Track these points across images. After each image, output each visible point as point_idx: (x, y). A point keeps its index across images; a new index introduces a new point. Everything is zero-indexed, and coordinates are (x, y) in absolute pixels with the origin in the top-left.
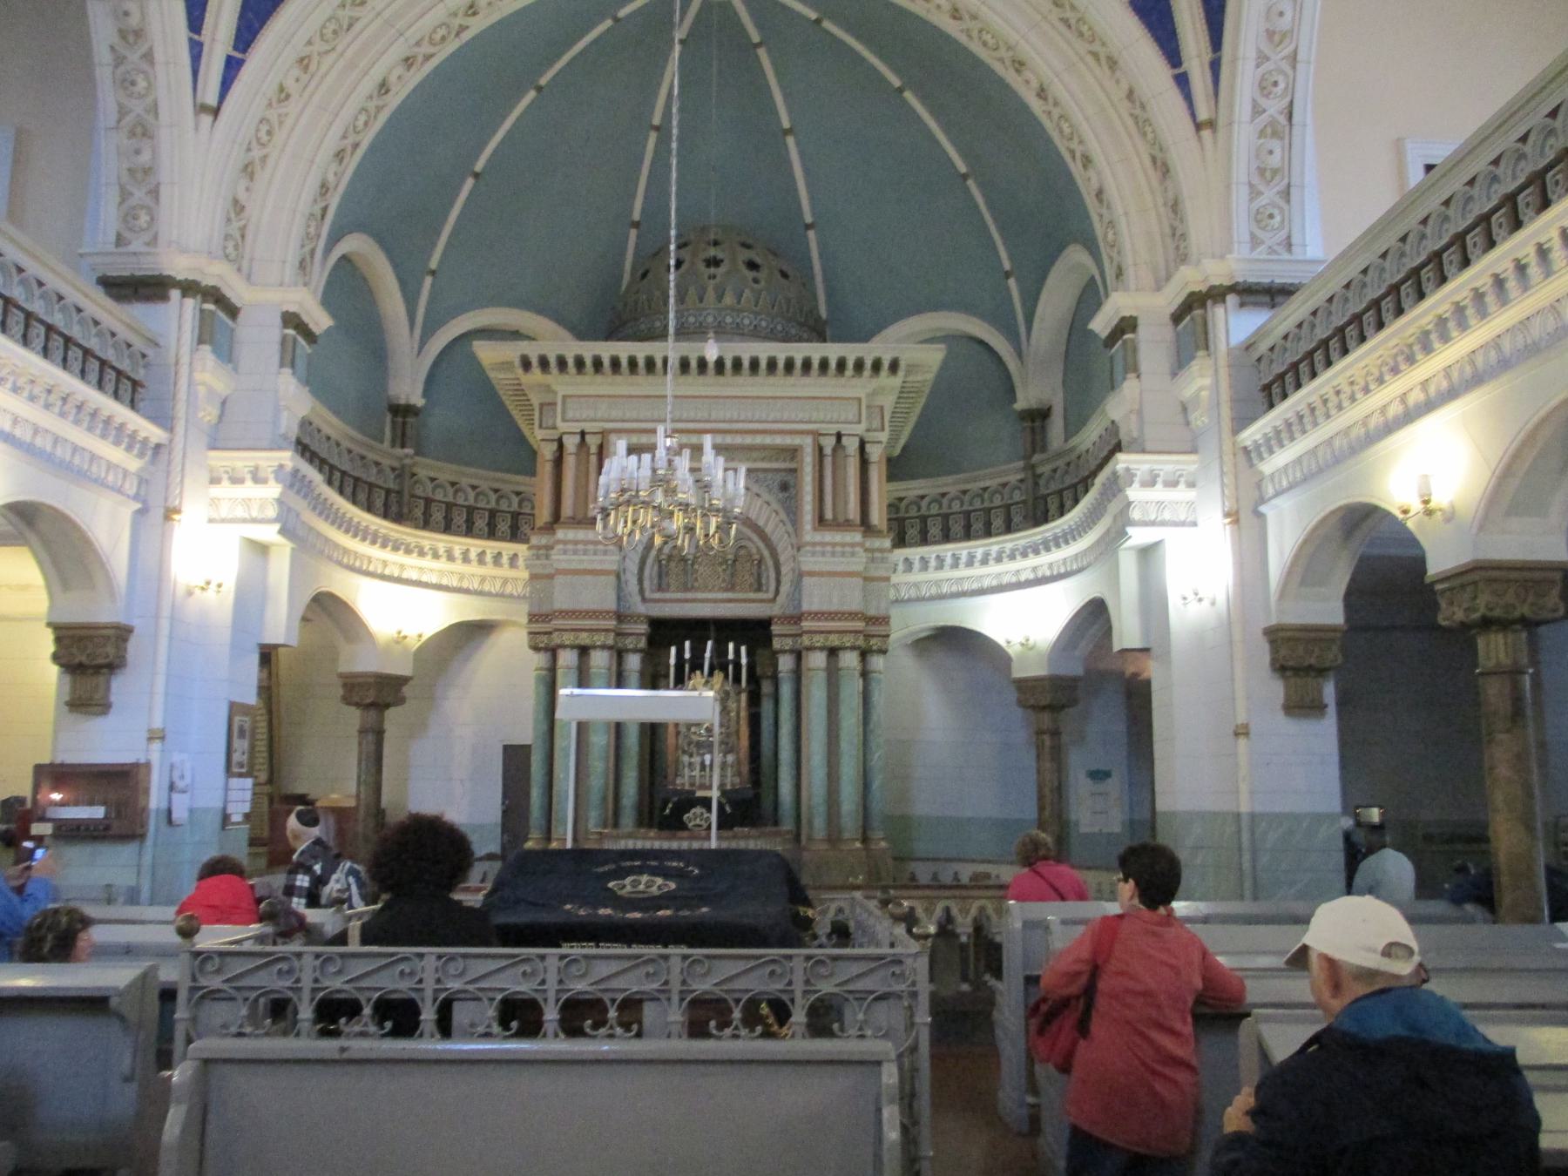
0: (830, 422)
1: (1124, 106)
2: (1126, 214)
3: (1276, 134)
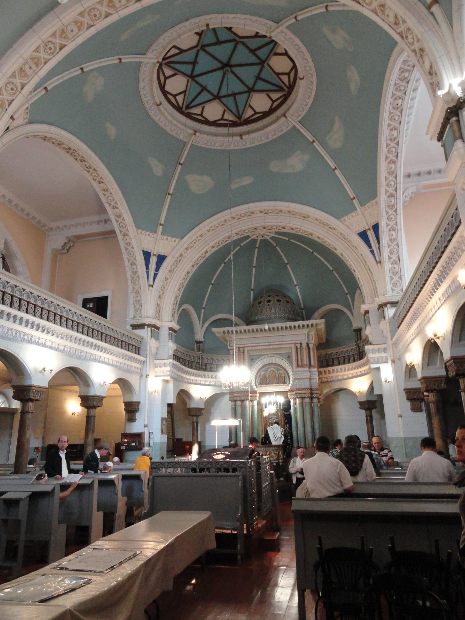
3: (396, 263)
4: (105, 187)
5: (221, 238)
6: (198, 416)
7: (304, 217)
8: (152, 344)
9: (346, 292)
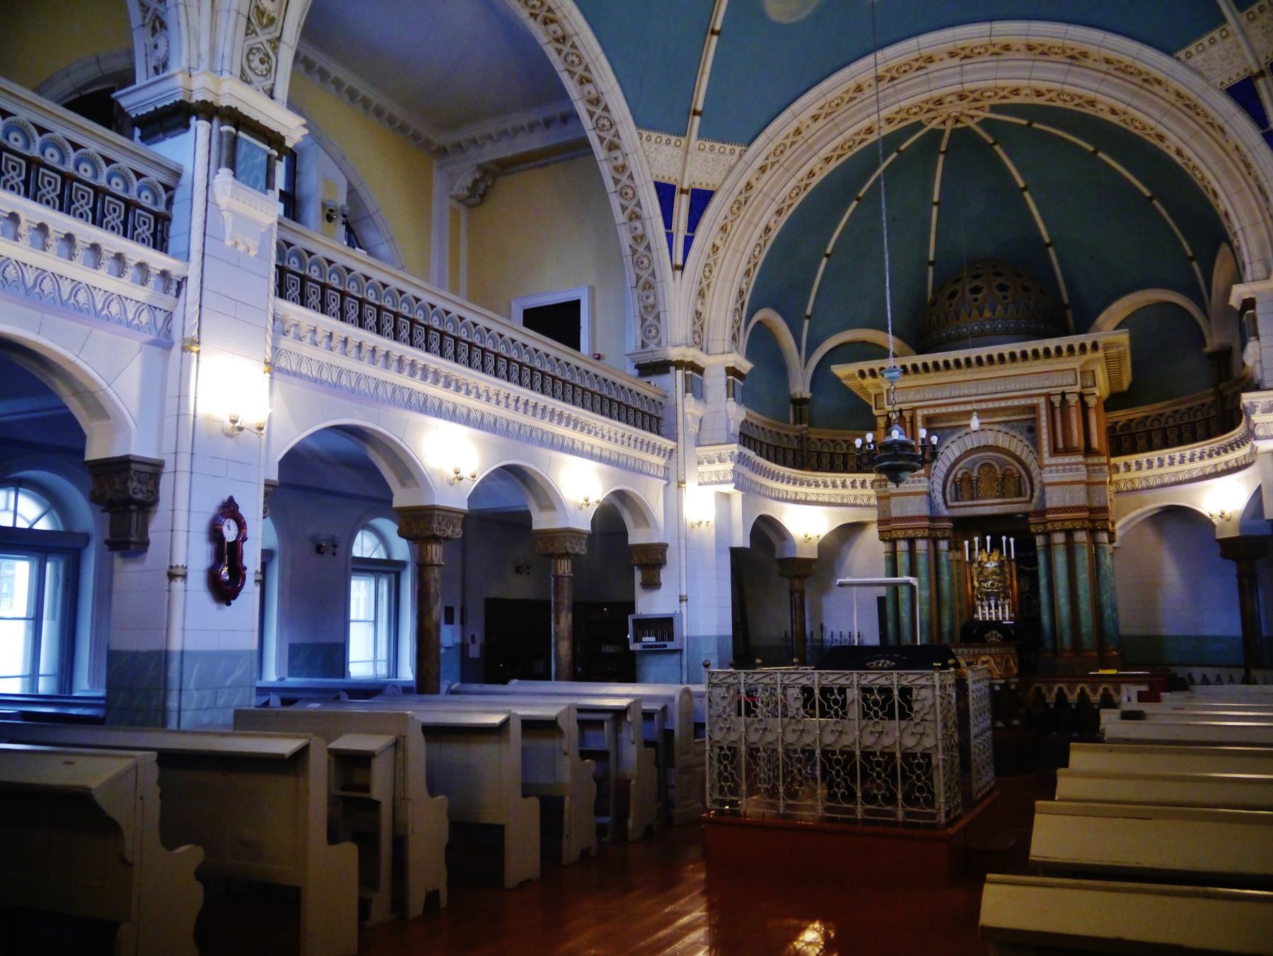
0: (1056, 387)
1: (1235, 155)
2: (1242, 229)
4: (560, 33)
5: (847, 134)
6: (802, 577)
7: (1072, 57)
8: (689, 409)
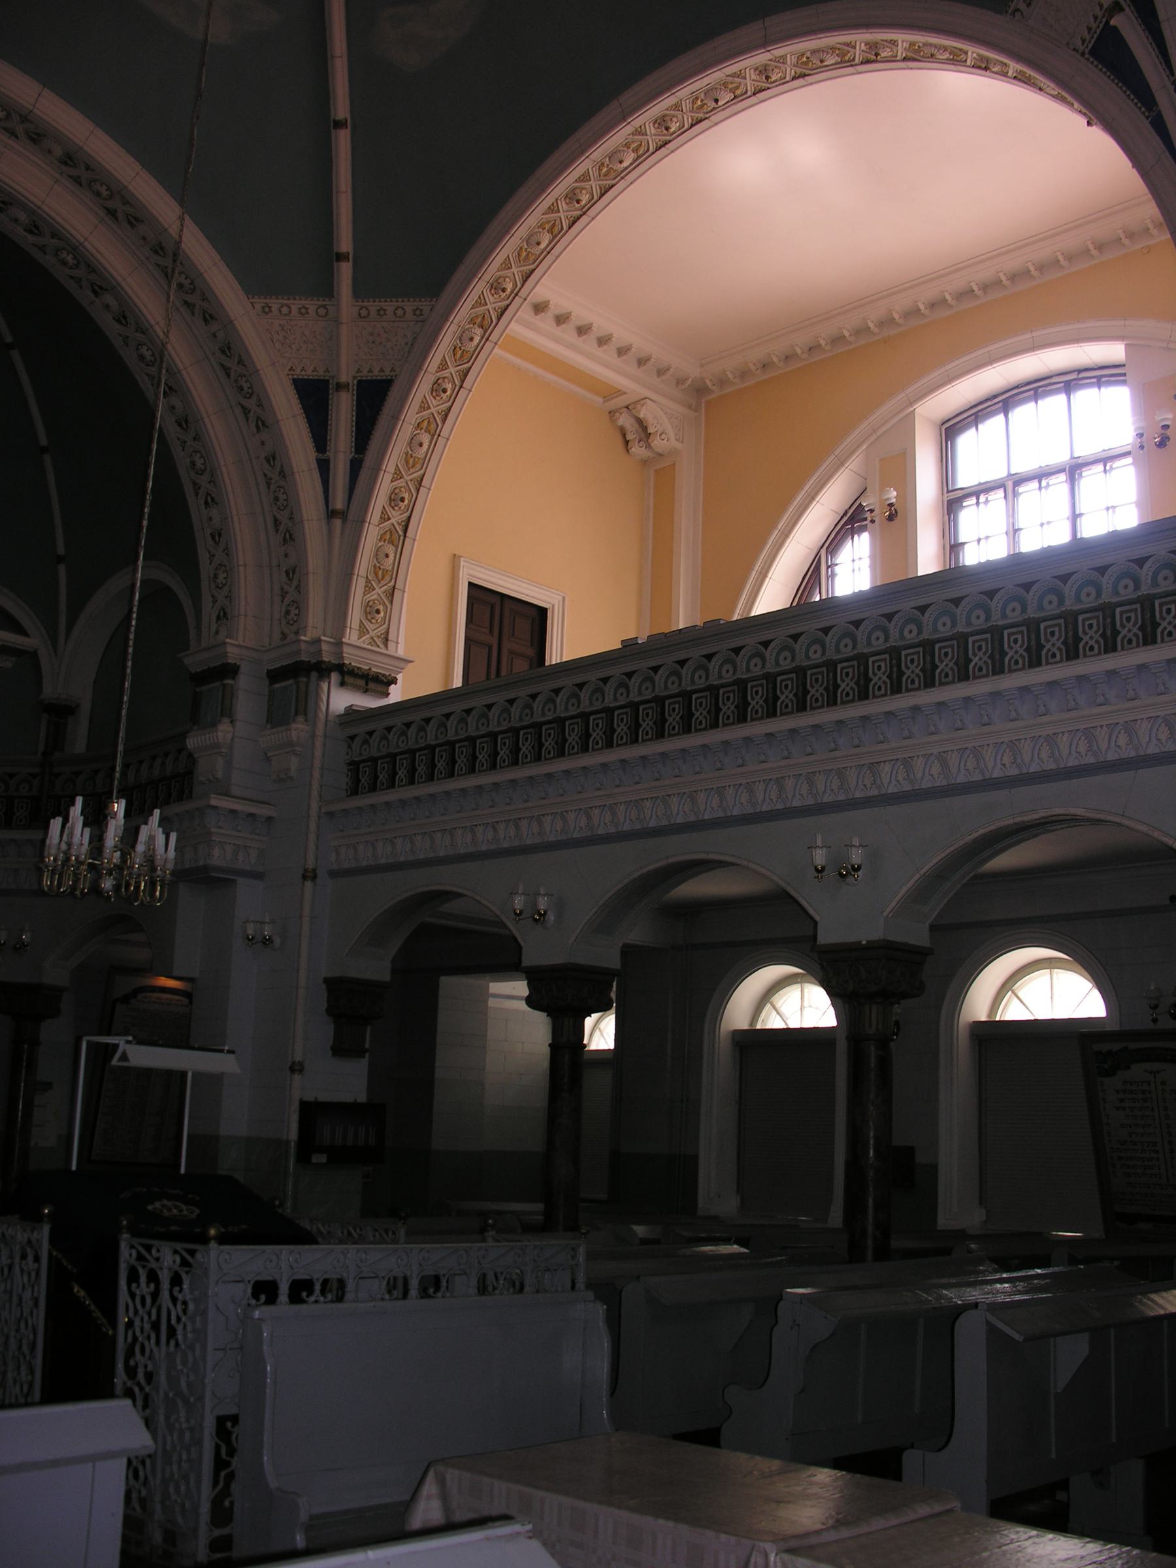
3: (391, 542)
9: (61, 550)
